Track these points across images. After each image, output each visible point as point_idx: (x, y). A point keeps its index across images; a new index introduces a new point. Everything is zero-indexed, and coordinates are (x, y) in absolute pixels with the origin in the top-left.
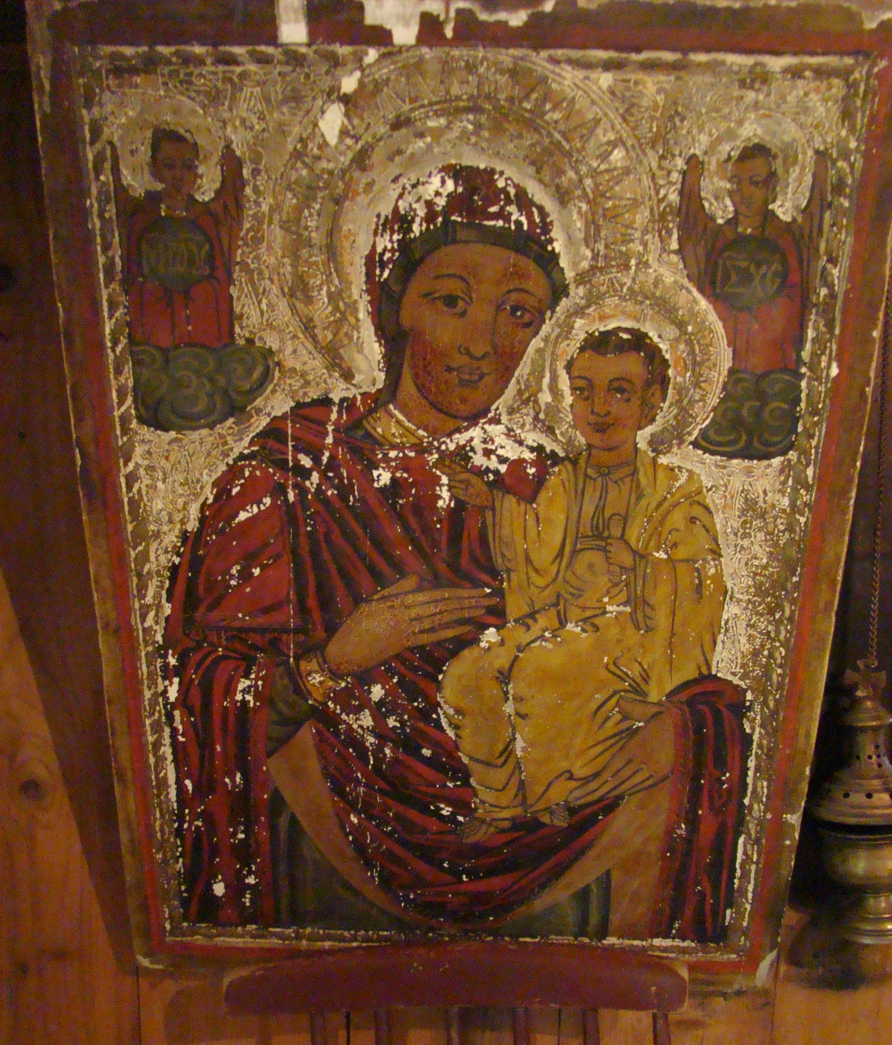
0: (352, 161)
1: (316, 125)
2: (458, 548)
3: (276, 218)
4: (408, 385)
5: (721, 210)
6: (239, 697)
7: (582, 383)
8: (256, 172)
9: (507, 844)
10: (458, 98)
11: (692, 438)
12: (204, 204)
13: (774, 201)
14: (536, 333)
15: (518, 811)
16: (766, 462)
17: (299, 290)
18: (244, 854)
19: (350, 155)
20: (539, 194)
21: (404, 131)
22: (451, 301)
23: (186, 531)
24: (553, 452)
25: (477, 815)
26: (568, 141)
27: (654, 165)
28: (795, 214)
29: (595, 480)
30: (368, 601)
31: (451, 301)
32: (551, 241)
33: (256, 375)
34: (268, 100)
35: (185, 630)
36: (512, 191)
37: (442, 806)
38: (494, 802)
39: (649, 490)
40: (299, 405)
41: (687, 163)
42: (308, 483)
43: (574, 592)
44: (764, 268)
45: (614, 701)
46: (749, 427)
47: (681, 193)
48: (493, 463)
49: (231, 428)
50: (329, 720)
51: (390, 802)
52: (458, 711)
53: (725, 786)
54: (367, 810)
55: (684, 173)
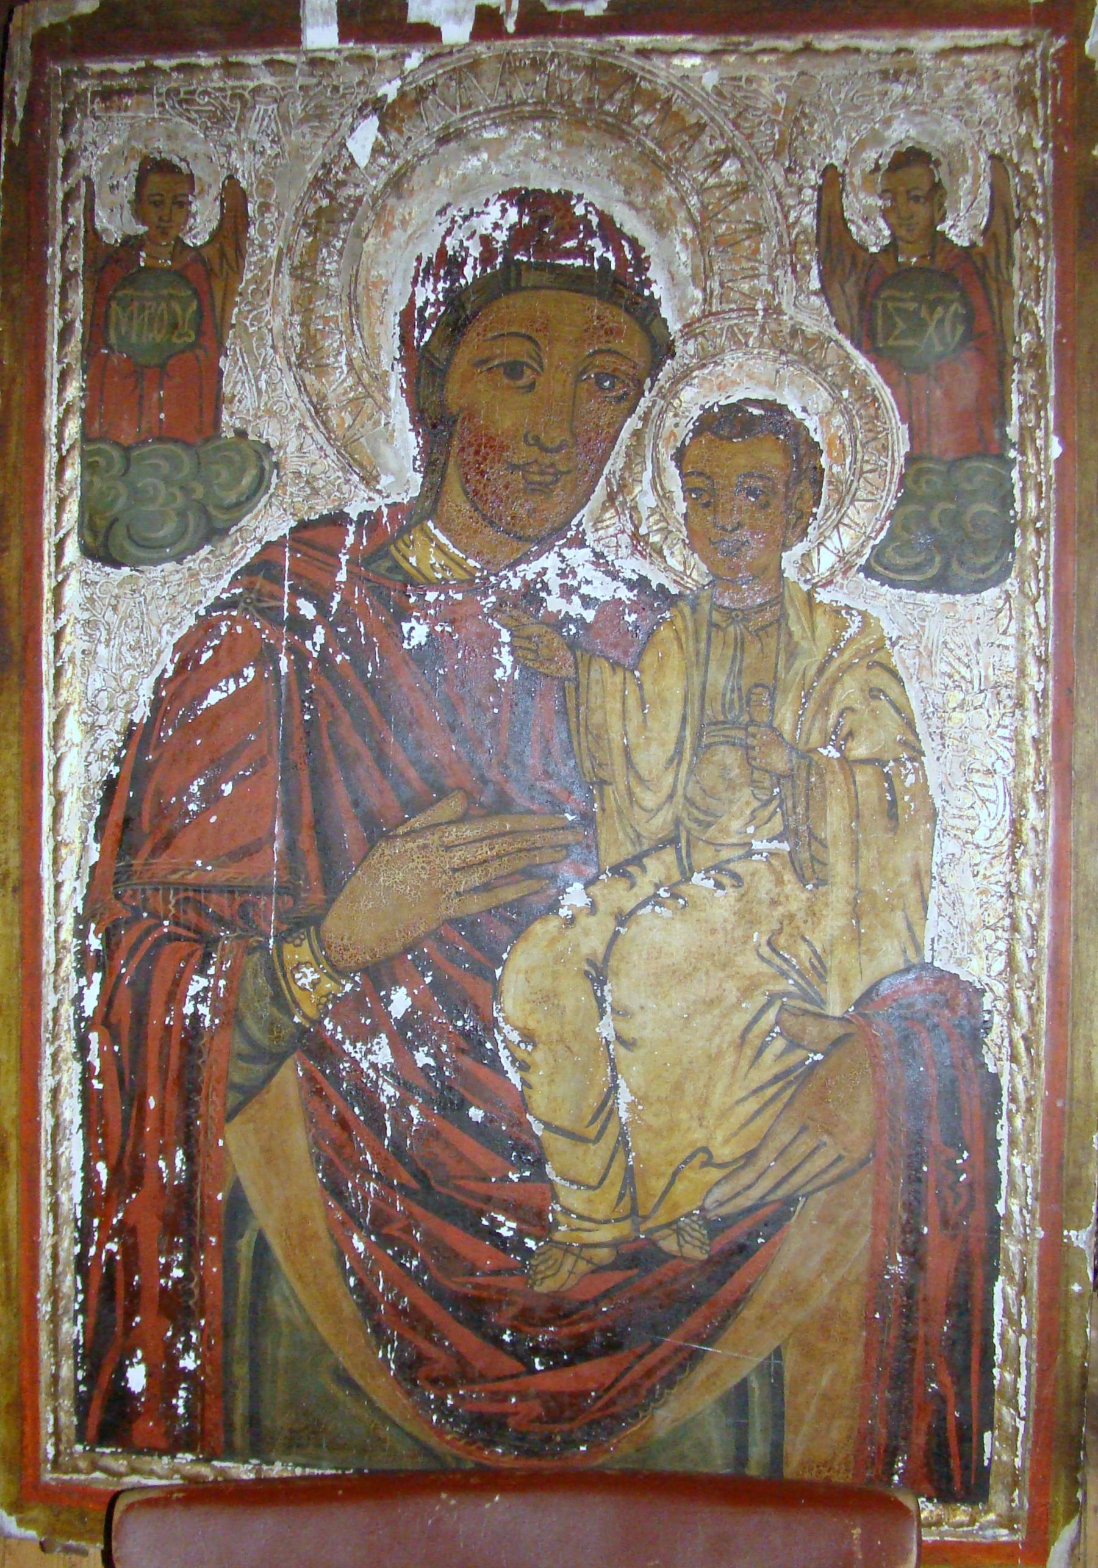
0: (386, 185)
1: (343, 145)
3: (286, 264)
4: (455, 497)
5: (873, 233)
6: (188, 1009)
7: (698, 482)
8: (264, 208)
9: (606, 1295)
10: (524, 103)
11: (862, 561)
12: (196, 248)
13: (943, 220)
14: (632, 410)
15: (624, 1229)
16: (974, 598)
17: (308, 357)
19: (384, 177)
20: (629, 222)
21: (453, 145)
22: (513, 370)
23: (132, 723)
24: (661, 586)
25: (557, 1236)
26: (664, 150)
27: (780, 180)
28: (973, 237)
29: (724, 630)
30: (387, 837)
31: (513, 370)
32: (648, 283)
33: (247, 481)
34: (284, 119)
36: (595, 220)
37: (501, 1218)
38: (586, 1213)
39: (804, 644)
40: (303, 525)
41: (823, 176)
42: (308, 644)
43: (701, 817)
44: (940, 310)
45: (771, 1015)
47: (818, 214)
48: (575, 607)
49: (207, 560)
50: (322, 1051)
51: (417, 1210)
52: (528, 1037)
53: (963, 1177)
54: (379, 1224)
55: (820, 189)
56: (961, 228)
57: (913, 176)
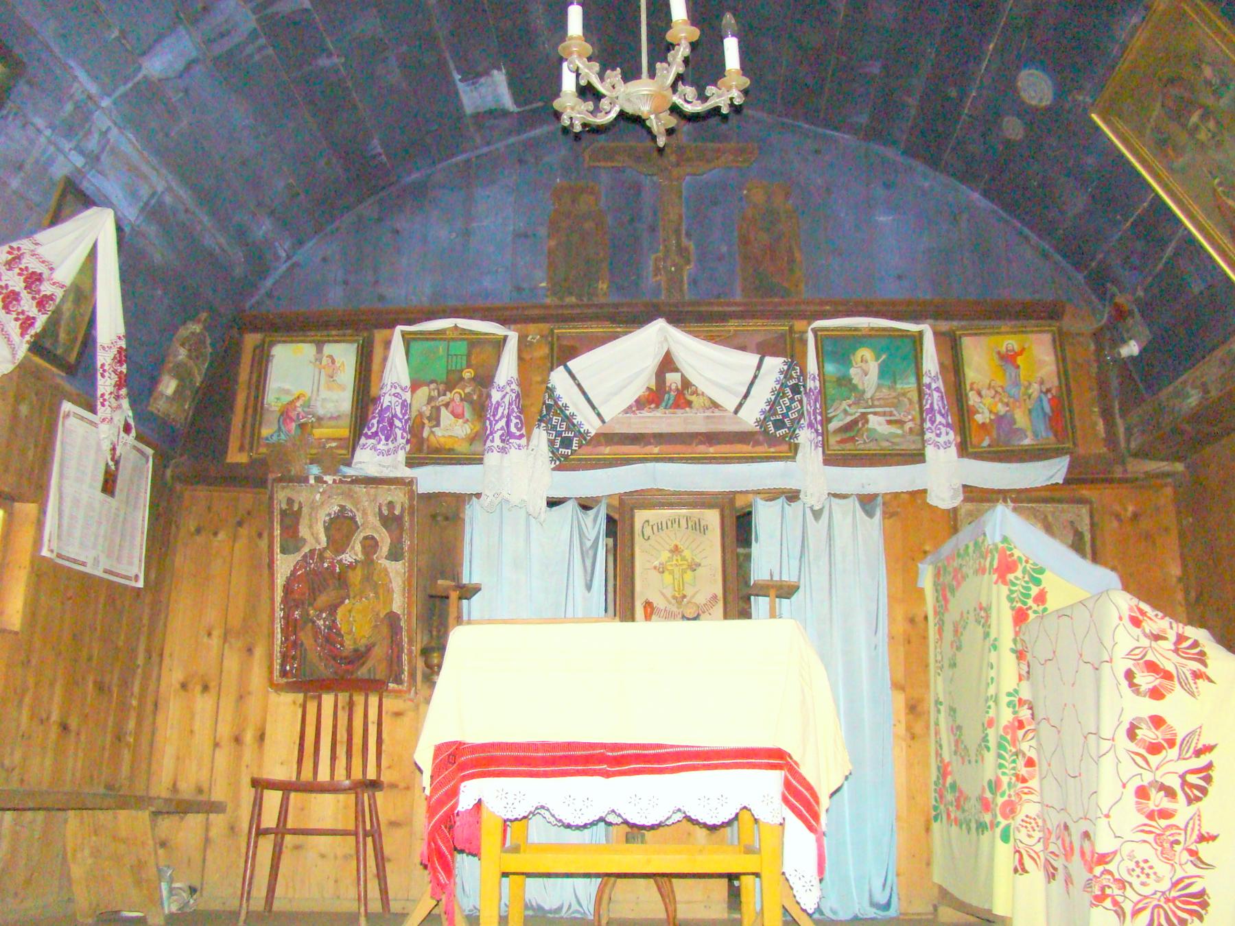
2: (341, 579)
5: (386, 513)
17: (311, 527)
18: (294, 658)
35: (285, 601)
38: (349, 644)
46: (394, 555)
50: (314, 622)
56: (397, 512)
57: (391, 505)
